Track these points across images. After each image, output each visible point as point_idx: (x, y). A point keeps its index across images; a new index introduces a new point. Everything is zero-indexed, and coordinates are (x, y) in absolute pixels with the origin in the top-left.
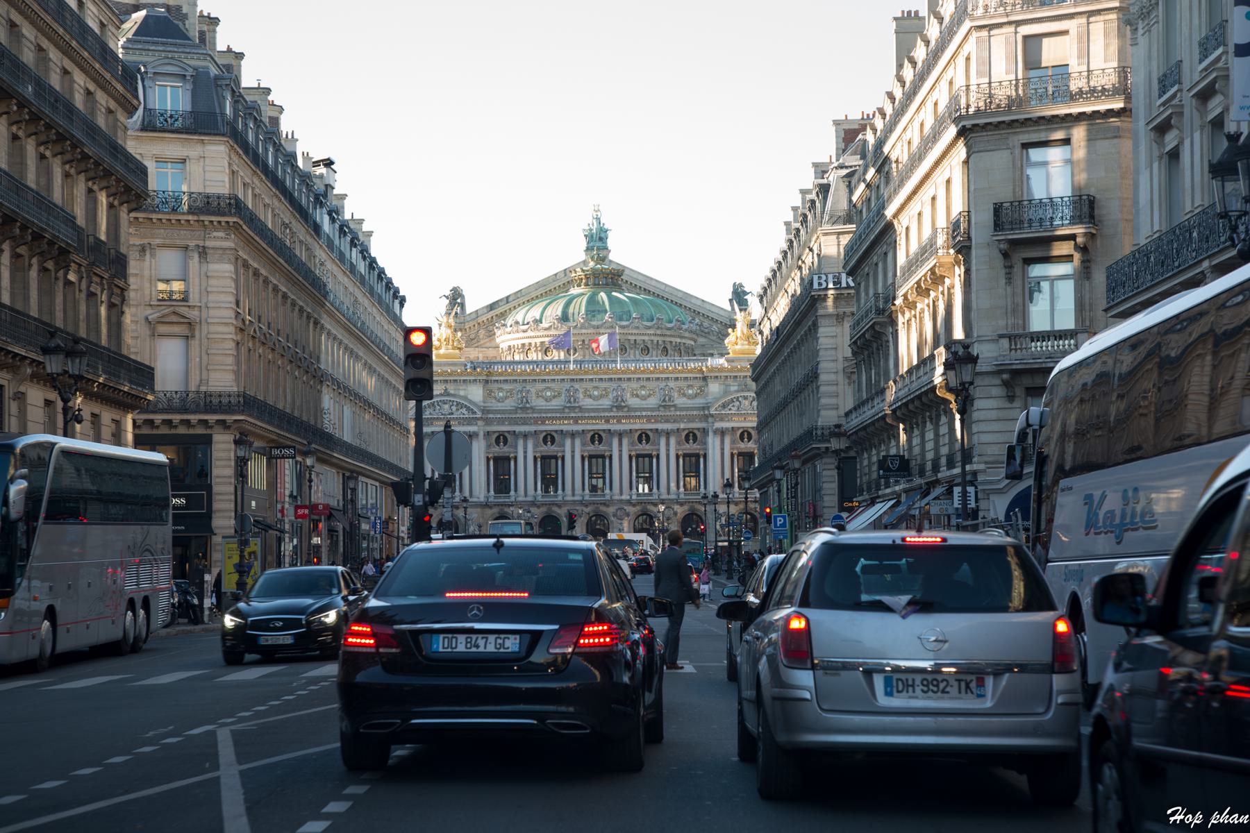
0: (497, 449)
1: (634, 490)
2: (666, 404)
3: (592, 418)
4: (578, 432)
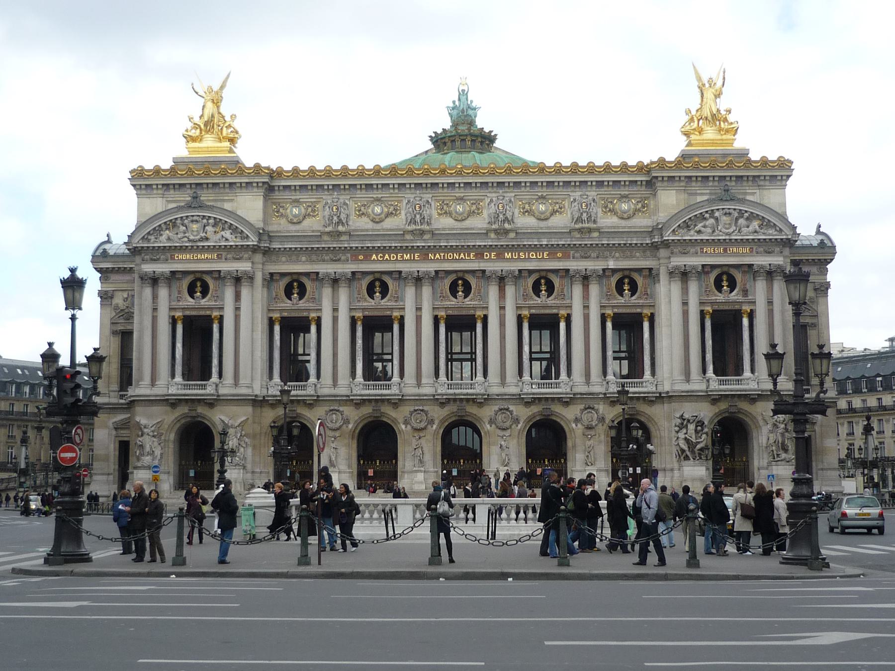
0: (287, 304)
2: (584, 227)
3: (452, 249)
4: (427, 273)
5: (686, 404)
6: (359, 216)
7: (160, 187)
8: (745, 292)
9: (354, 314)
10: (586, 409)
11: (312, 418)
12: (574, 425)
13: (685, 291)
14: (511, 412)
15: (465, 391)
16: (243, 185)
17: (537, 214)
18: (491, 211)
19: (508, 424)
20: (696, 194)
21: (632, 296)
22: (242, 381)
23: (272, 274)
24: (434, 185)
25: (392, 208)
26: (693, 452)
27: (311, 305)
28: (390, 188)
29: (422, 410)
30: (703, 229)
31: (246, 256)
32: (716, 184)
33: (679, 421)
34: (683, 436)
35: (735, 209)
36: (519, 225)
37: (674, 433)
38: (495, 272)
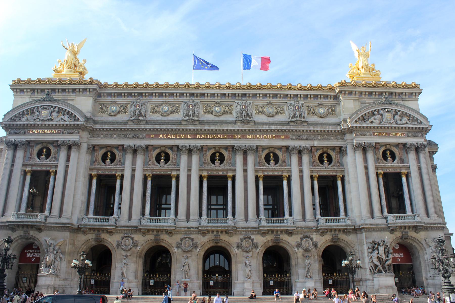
0: (102, 166)
1: (262, 216)
4: (196, 147)
5: (374, 233)
6: (153, 112)
7: (28, 90)
8: (402, 161)
9: (145, 173)
10: (304, 238)
11: (112, 242)
12: (296, 249)
13: (365, 160)
14: (252, 240)
15: (220, 225)
16: (81, 90)
17: (267, 113)
18: (238, 110)
19: (250, 248)
20: (365, 103)
21: (329, 164)
22: (64, 214)
23: (94, 146)
24: (202, 95)
25: (174, 108)
26: (384, 267)
27: (118, 167)
28: (173, 96)
29: (190, 238)
30: (374, 121)
31: (76, 132)
32: (377, 97)
33: (371, 246)
34: (376, 256)
35: (392, 109)
36: (255, 120)
37: (366, 254)
38: (240, 147)
